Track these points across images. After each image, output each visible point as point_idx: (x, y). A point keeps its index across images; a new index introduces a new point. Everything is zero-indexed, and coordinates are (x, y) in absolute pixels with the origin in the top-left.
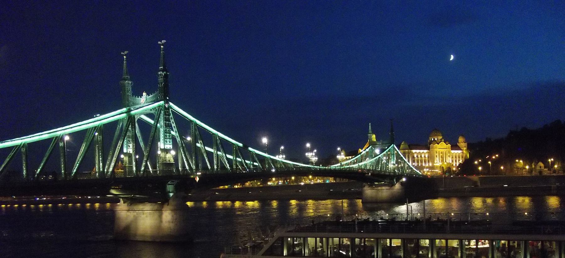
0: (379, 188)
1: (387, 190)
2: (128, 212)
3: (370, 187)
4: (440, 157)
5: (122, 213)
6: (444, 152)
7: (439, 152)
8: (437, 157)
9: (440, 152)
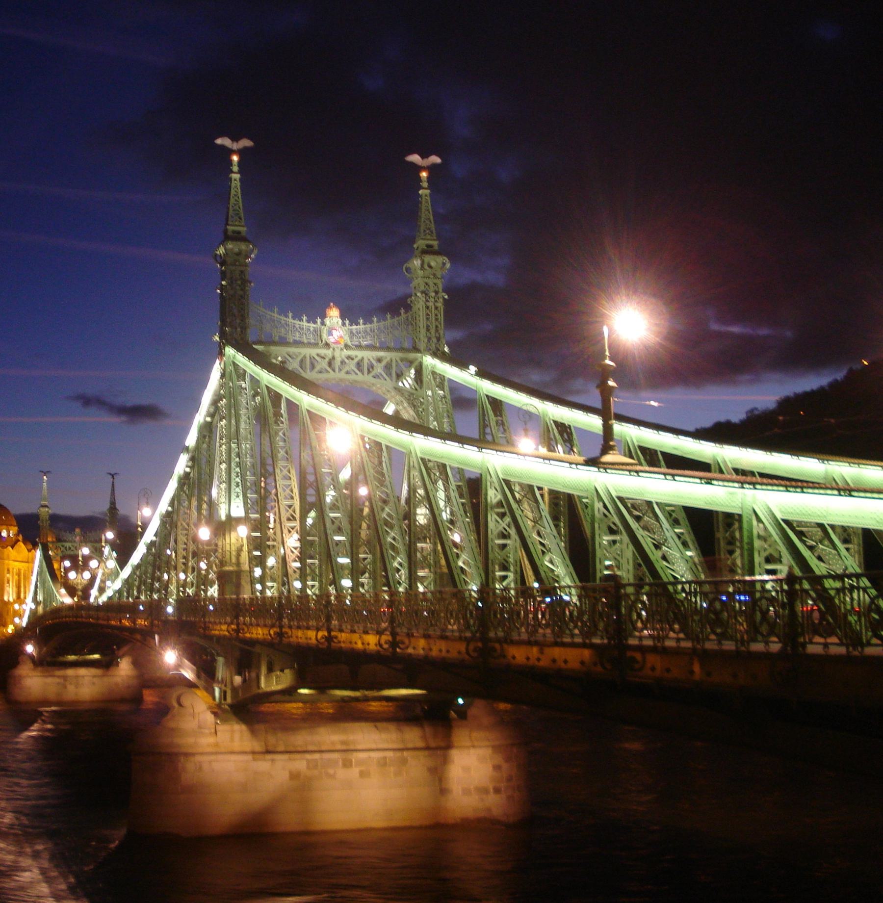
0: (70, 672)
1: (95, 680)
2: (254, 759)
3: (40, 669)
4: (14, 584)
5: (216, 766)
6: (22, 572)
7: (13, 569)
8: (8, 582)
9: (15, 570)
